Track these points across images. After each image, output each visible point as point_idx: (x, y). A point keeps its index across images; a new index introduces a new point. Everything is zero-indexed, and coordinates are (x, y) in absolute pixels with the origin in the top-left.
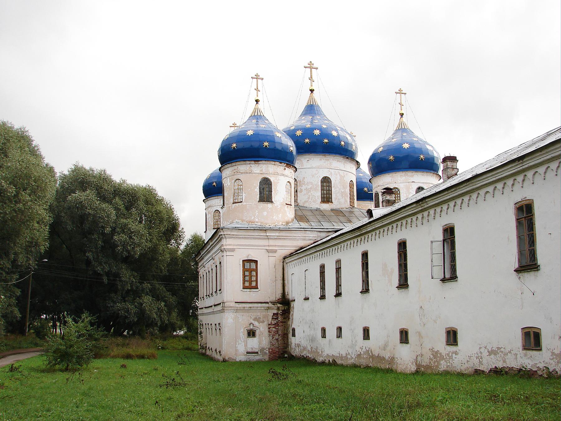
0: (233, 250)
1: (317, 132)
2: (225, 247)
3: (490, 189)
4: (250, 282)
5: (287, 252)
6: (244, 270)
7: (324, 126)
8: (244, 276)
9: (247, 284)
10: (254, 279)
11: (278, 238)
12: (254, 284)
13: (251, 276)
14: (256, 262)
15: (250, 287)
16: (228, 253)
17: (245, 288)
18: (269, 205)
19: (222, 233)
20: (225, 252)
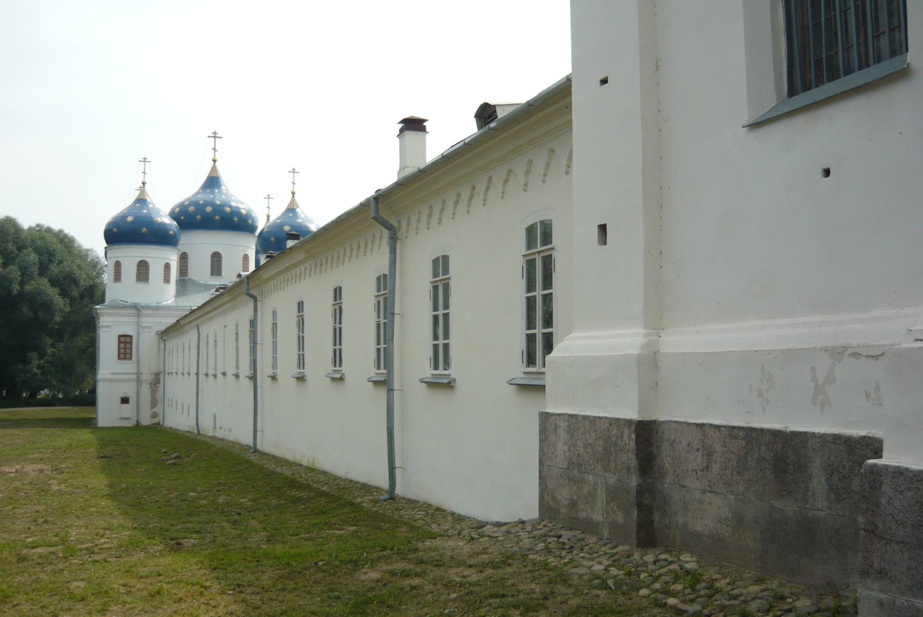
0: (109, 327)
1: (209, 209)
4: (125, 353)
5: (163, 328)
6: (119, 342)
7: (218, 202)
8: (119, 348)
9: (122, 356)
11: (151, 316)
12: (128, 356)
13: (125, 348)
14: (131, 337)
15: (125, 358)
17: (119, 358)
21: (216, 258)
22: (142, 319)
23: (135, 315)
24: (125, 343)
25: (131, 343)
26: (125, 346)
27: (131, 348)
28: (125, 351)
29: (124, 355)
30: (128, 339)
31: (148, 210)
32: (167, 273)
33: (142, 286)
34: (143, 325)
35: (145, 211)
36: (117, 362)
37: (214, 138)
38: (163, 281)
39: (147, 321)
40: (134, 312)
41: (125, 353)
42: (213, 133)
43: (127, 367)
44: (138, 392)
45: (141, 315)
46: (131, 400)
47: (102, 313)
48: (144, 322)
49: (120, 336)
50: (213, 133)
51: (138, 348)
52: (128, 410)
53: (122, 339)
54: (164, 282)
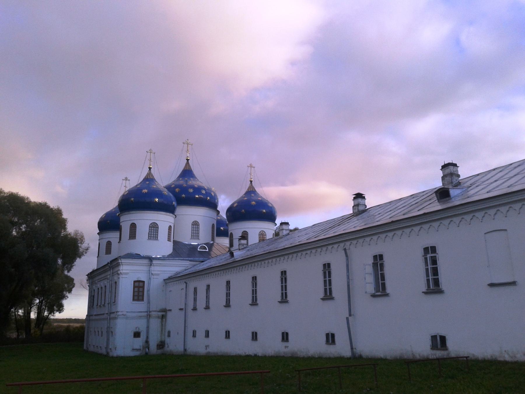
2: (121, 271)
3: (309, 252)
6: (134, 287)
8: (134, 292)
9: (136, 298)
10: (141, 294)
11: (160, 265)
12: (140, 298)
13: (139, 292)
14: (144, 282)
15: (138, 300)
16: (124, 276)
17: (134, 300)
18: (155, 242)
19: (120, 261)
20: (121, 275)
22: (152, 268)
23: (148, 264)
24: (139, 287)
25: (143, 287)
27: (143, 292)
29: (137, 297)
30: (141, 284)
31: (156, 186)
32: (170, 234)
33: (153, 242)
34: (153, 272)
35: (155, 187)
36: (132, 303)
38: (167, 239)
39: (156, 269)
40: (146, 261)
41: (138, 296)
43: (141, 306)
44: (148, 327)
45: (152, 265)
46: (142, 334)
47: (122, 263)
48: (154, 271)
49: (135, 282)
52: (139, 343)
53: (137, 284)
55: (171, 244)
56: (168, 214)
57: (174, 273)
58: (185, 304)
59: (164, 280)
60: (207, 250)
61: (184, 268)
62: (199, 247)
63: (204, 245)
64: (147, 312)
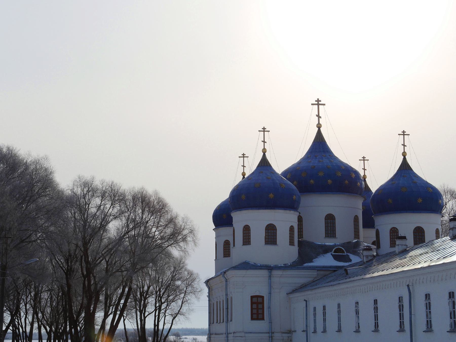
4: (258, 314)
6: (252, 303)
8: (252, 309)
9: (255, 316)
10: (260, 311)
12: (260, 316)
13: (258, 309)
14: (263, 297)
15: (258, 319)
17: (252, 319)
21: (330, 219)
24: (257, 303)
25: (263, 303)
26: (257, 306)
28: (258, 311)
30: (260, 300)
37: (317, 106)
40: (265, 273)
41: (258, 314)
42: (316, 101)
49: (252, 297)
50: (316, 101)
51: (269, 308)
53: (255, 300)
54: (290, 245)
55: (295, 250)
56: (288, 211)
57: (299, 285)
58: (307, 326)
59: (287, 294)
60: (345, 253)
61: (312, 279)
62: (334, 250)
63: (339, 247)
64: (269, 333)
